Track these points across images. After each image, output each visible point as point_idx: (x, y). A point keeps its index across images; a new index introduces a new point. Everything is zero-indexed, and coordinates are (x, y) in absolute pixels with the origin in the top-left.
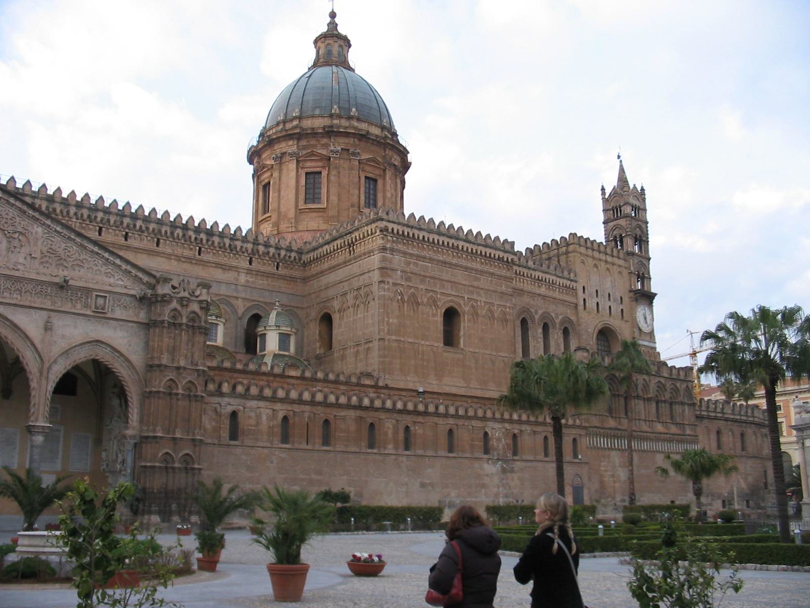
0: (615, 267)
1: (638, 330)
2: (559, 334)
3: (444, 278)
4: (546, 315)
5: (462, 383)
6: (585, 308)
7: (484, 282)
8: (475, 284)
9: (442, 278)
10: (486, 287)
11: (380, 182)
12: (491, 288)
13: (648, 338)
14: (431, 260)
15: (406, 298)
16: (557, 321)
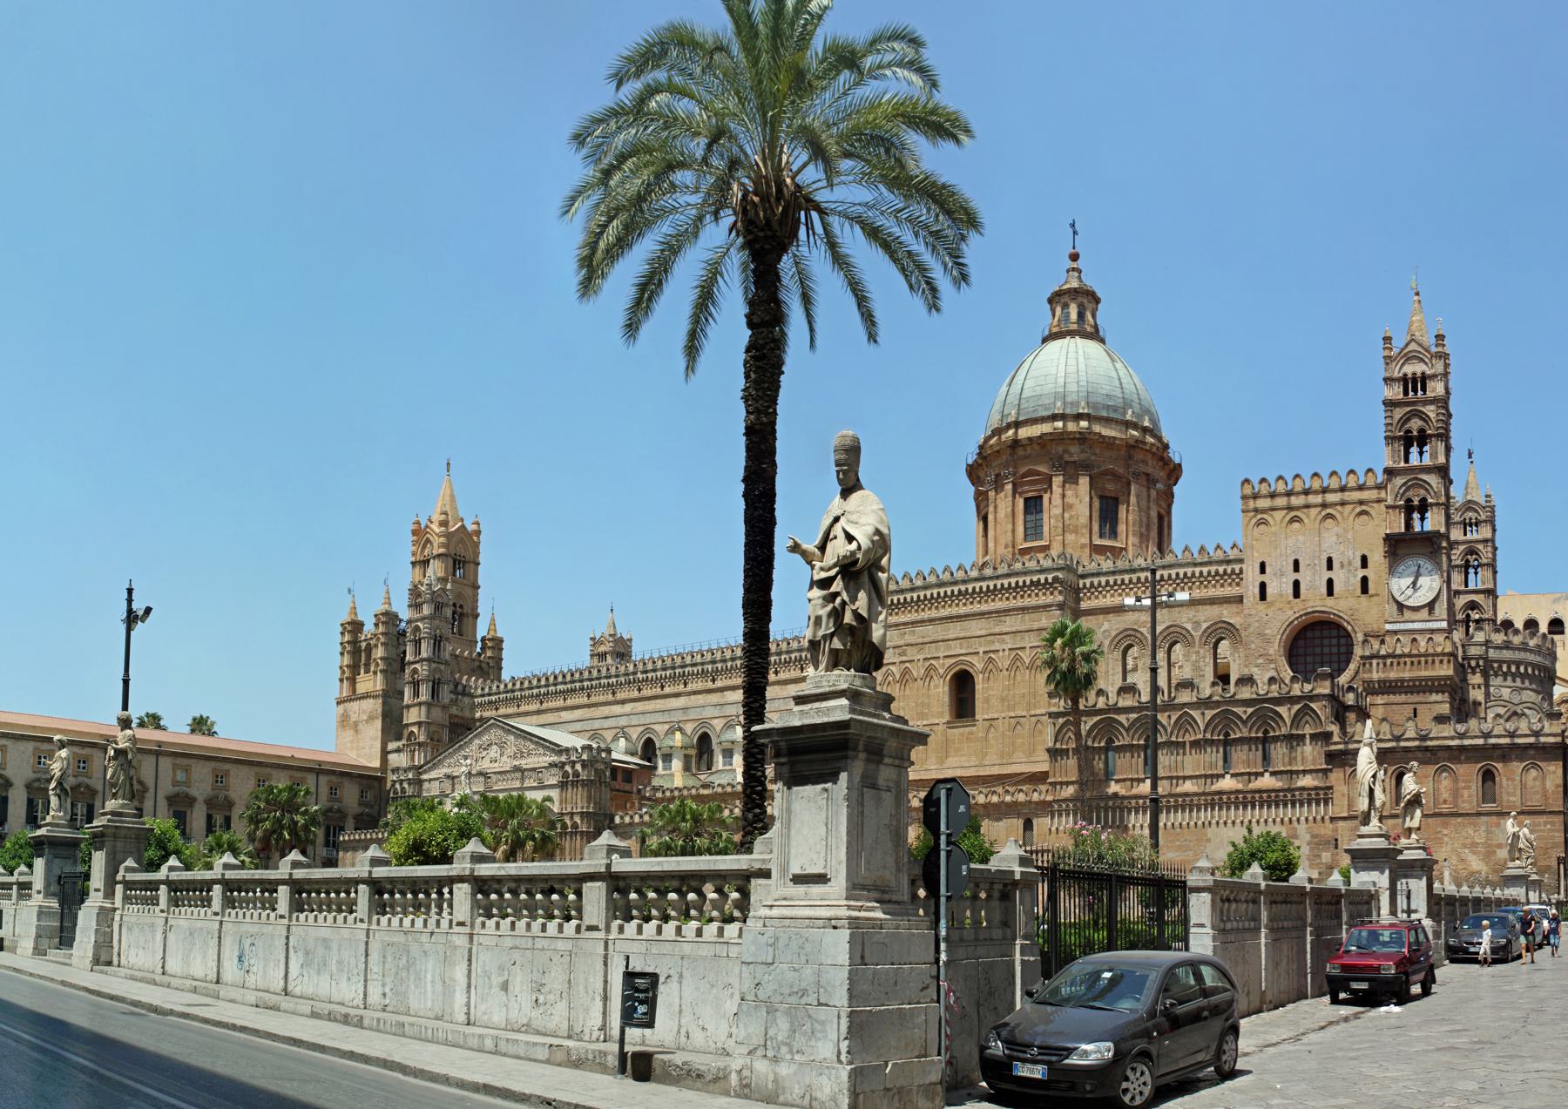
0: (1349, 508)
1: (1395, 607)
2: (1202, 651)
3: (951, 636)
4: (1172, 630)
5: (974, 761)
6: (1263, 596)
7: (1011, 623)
8: (997, 630)
9: (946, 637)
10: (1014, 629)
11: (1046, 497)
12: (1023, 628)
13: (1424, 614)
14: (931, 621)
15: (898, 677)
16: (1197, 635)
